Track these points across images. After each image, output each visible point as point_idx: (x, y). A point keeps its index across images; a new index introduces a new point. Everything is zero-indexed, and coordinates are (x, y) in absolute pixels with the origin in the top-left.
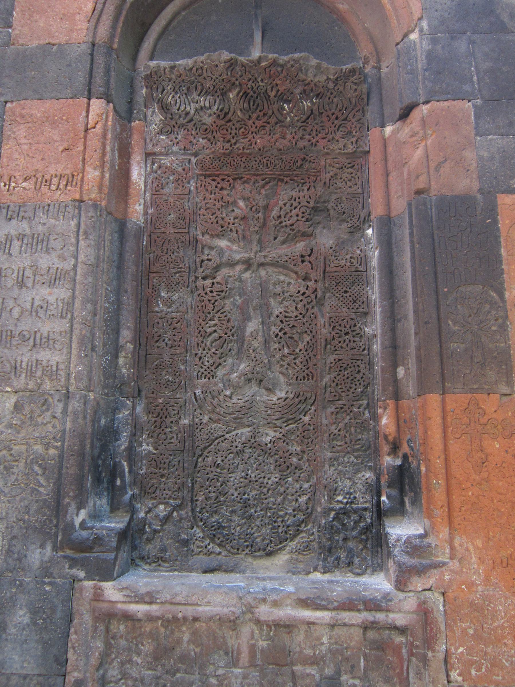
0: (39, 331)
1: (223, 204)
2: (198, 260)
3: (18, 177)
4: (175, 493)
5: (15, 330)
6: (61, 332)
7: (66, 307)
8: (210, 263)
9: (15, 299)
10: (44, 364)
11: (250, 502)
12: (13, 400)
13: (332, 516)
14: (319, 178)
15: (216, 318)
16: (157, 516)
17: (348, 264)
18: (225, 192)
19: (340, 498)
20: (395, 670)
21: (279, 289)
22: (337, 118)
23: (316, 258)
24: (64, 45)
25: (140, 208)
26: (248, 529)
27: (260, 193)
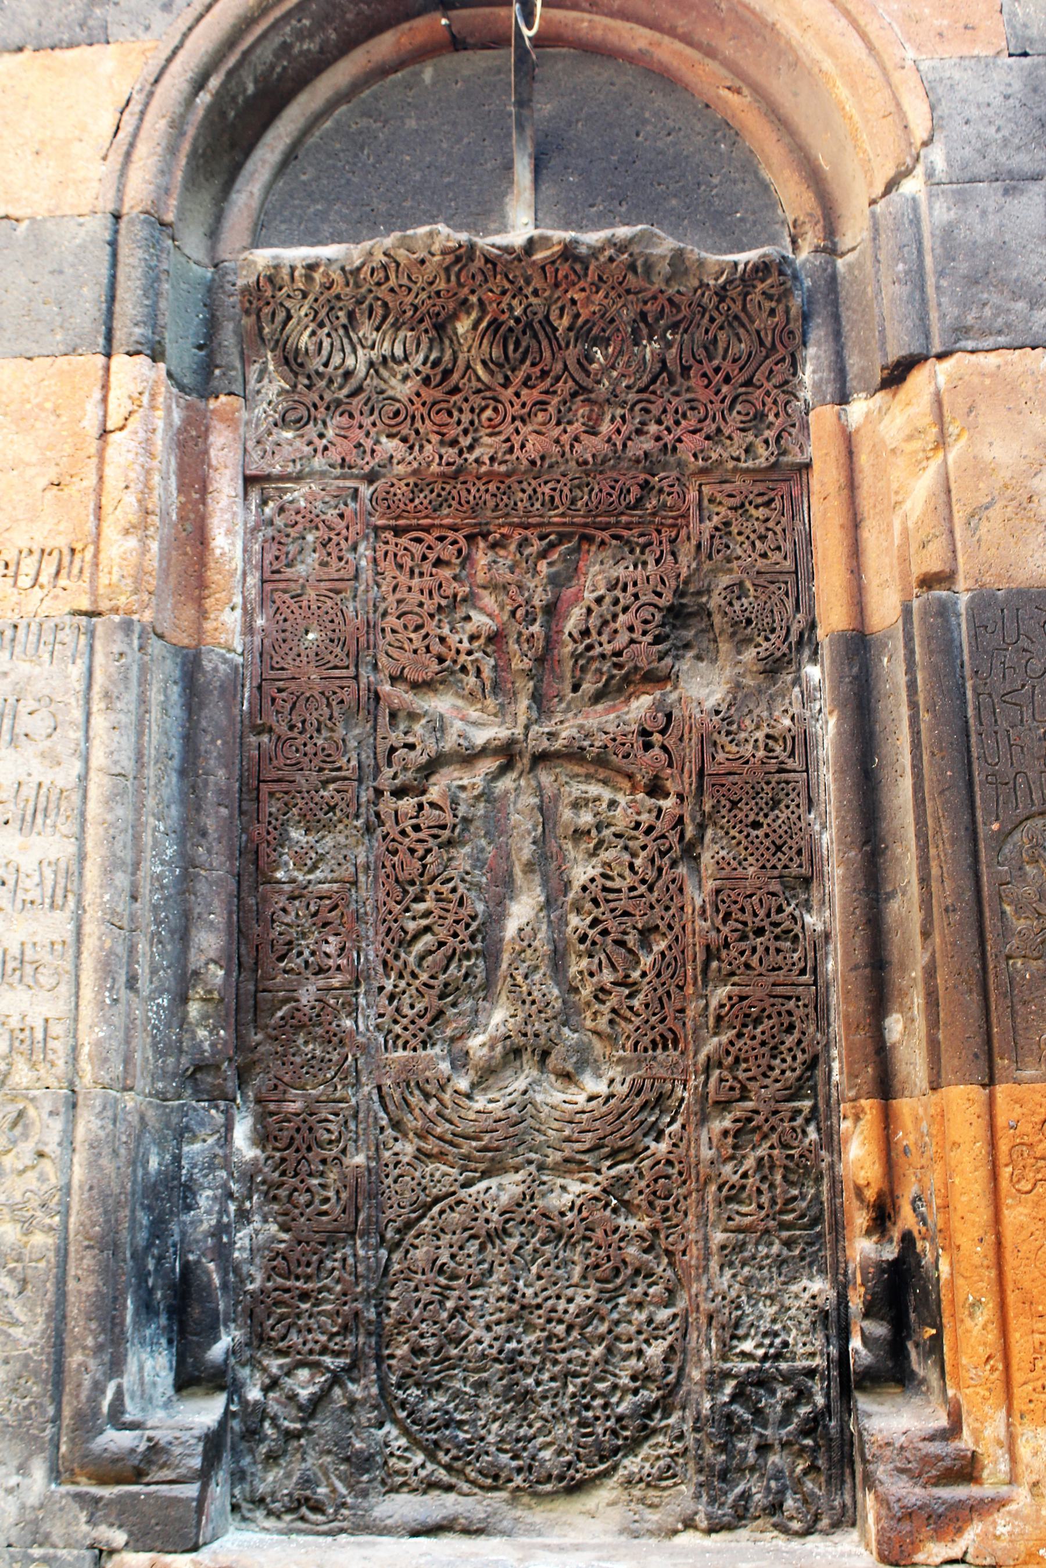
1: (444, 602)
2: (382, 748)
4: (338, 1339)
7: (62, 882)
8: (412, 754)
11: (522, 1359)
13: (728, 1390)
14: (683, 532)
15: (430, 896)
16: (293, 1397)
17: (761, 753)
18: (446, 573)
19: (747, 1346)
21: (586, 818)
22: (727, 380)
23: (681, 739)
24: (45, 220)
25: (232, 619)
26: (520, 1426)
27: (536, 572)
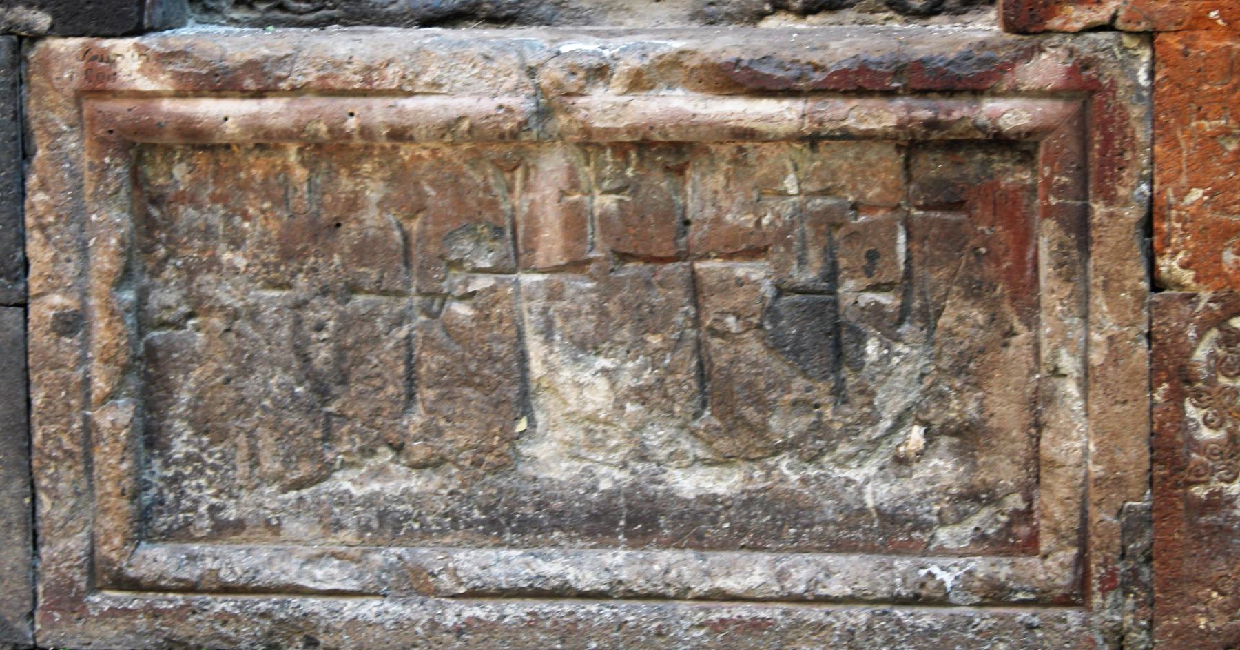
20: (998, 263)
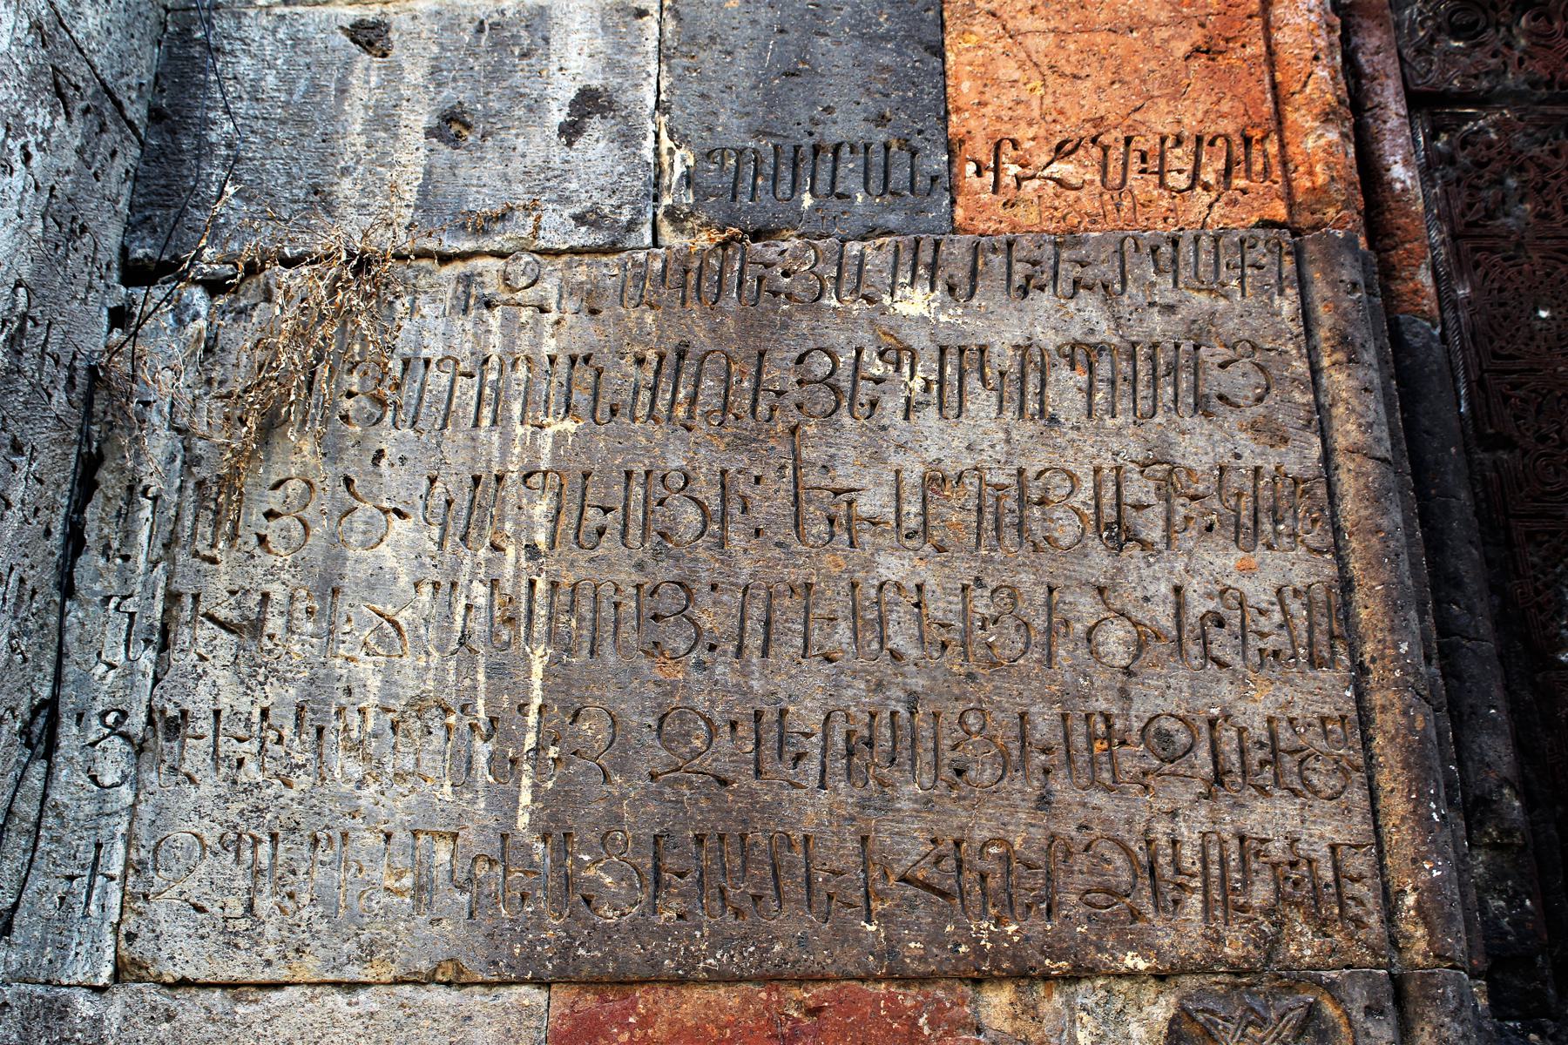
0: (1227, 718)
3: (1027, 145)
5: (1127, 718)
6: (1323, 720)
9: (1101, 590)
10: (1277, 850)
12: (1161, 1010)
